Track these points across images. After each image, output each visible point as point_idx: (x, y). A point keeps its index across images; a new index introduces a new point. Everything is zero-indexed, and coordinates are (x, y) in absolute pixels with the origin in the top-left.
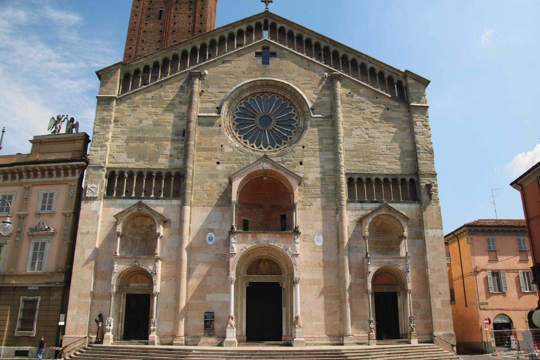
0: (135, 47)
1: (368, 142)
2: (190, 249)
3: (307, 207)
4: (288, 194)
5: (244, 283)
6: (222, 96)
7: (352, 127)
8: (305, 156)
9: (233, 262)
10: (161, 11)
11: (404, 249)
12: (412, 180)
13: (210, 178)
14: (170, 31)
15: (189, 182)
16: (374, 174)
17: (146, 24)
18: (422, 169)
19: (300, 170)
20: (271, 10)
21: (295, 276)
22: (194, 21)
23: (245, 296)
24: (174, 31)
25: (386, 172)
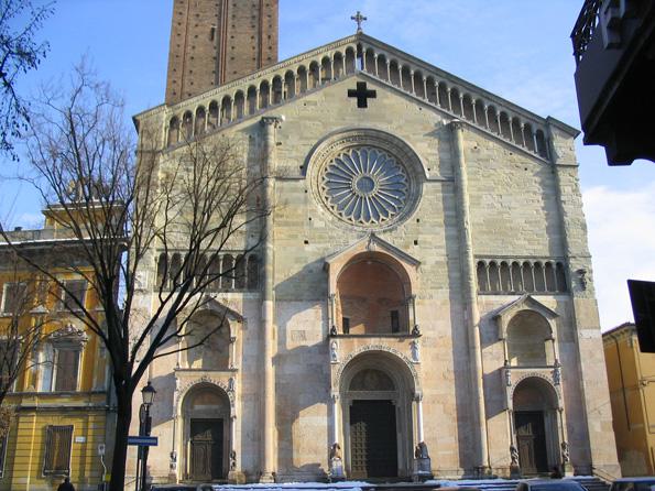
0: (180, 82)
1: (500, 213)
2: (277, 360)
3: (427, 301)
4: (403, 282)
5: (347, 401)
6: (308, 149)
7: (480, 193)
8: (419, 233)
9: (336, 373)
10: (213, 29)
11: (553, 351)
12: (559, 264)
13: (296, 262)
14: (228, 59)
15: (269, 268)
16: (512, 257)
17: (194, 47)
18: (573, 250)
19: (413, 252)
20: (365, 32)
21: (417, 392)
22: (260, 43)
23: (348, 419)
24: (233, 59)
25: (526, 254)
